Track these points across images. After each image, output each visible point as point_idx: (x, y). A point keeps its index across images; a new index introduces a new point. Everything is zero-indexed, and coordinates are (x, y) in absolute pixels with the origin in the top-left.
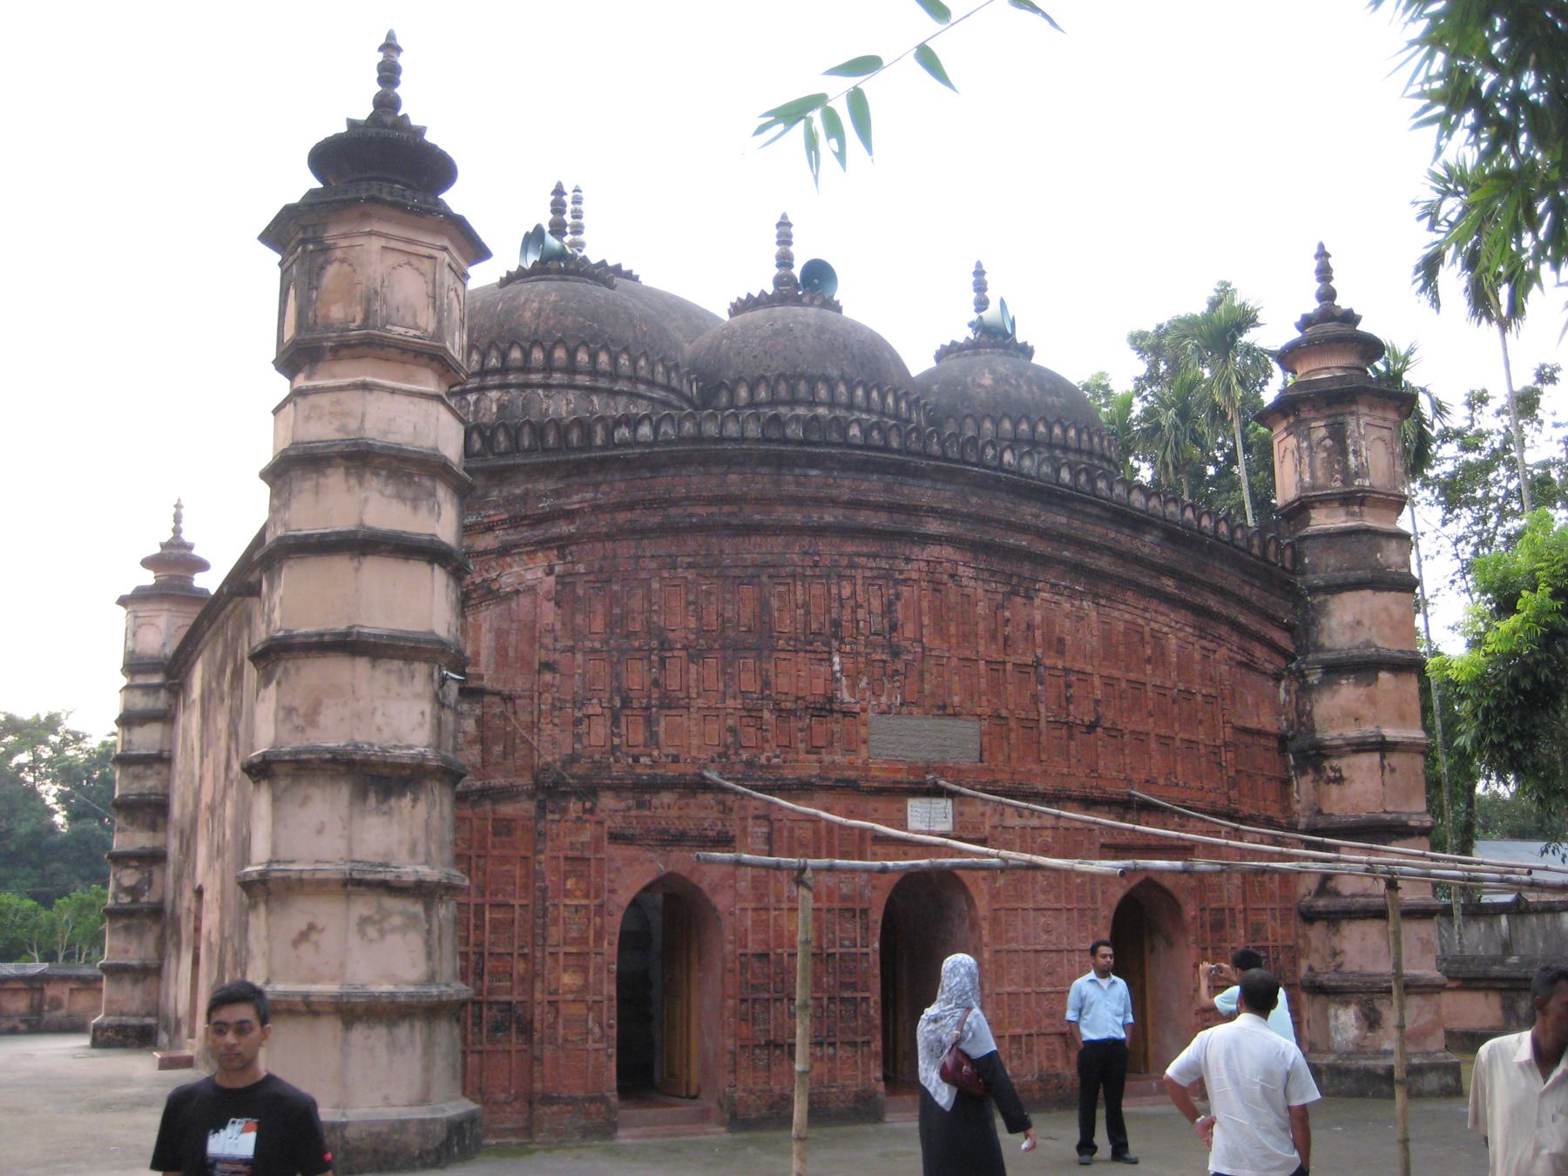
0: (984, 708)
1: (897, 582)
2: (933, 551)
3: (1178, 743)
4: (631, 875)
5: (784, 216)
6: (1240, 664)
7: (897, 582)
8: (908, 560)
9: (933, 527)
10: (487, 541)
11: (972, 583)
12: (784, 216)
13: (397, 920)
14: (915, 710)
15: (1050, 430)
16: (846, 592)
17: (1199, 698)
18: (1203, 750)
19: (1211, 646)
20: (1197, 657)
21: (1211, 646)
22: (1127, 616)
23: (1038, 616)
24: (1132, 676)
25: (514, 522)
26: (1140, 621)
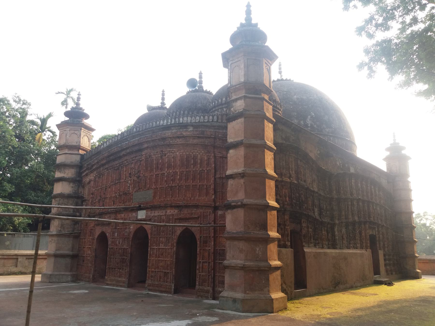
0: (154, 186)
1: (141, 161)
2: (146, 151)
3: (198, 186)
4: (98, 232)
5: (201, 72)
6: (221, 157)
7: (141, 161)
8: (142, 155)
9: (146, 146)
10: (85, 173)
11: (154, 156)
12: (201, 72)
13: (53, 241)
14: (141, 190)
15: (218, 101)
16: (132, 166)
17: (206, 171)
18: (205, 187)
19: (210, 154)
20: (206, 158)
21: (210, 154)
22: (187, 153)
23: (167, 160)
24: (188, 170)
25: (88, 169)
26: (191, 153)
